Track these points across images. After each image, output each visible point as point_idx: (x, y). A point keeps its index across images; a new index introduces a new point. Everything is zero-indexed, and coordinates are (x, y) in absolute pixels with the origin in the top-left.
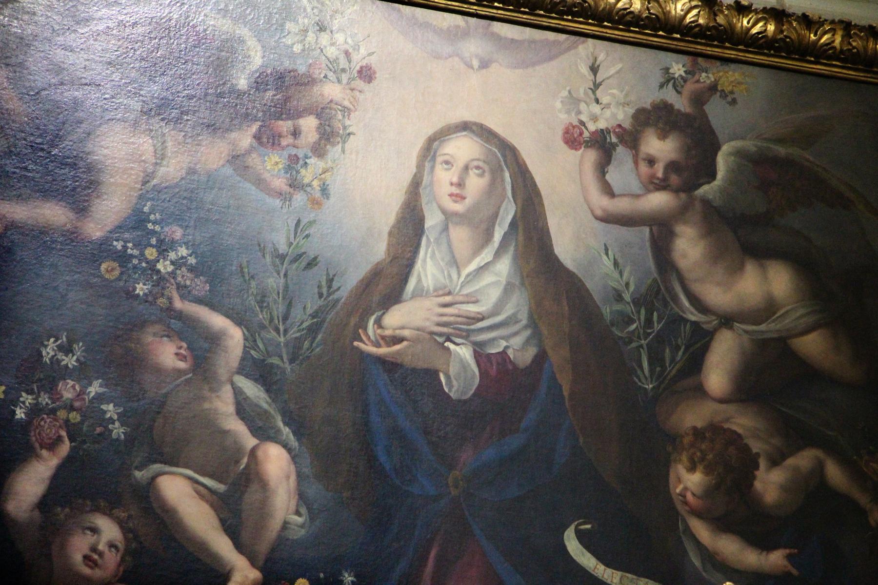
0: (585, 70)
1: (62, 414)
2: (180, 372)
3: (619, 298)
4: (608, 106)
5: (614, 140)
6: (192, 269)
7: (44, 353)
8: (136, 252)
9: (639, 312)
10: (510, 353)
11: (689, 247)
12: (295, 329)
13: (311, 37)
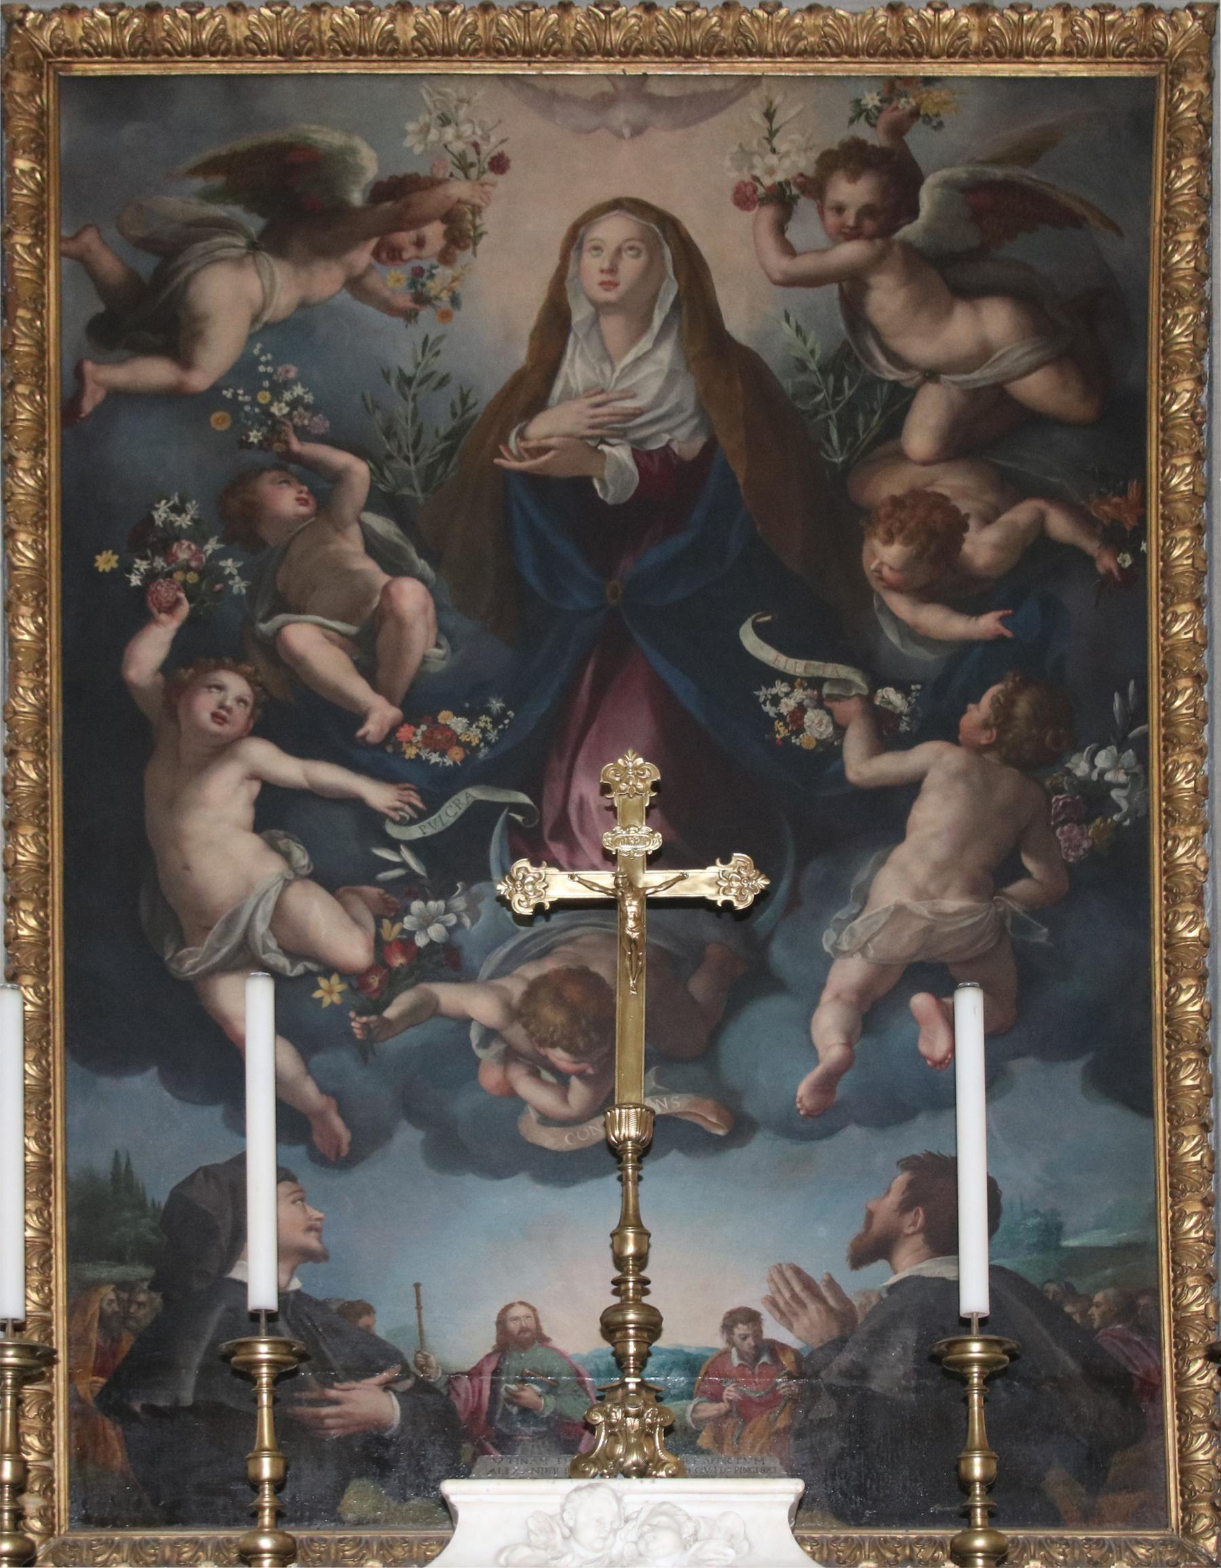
0: (758, 118)
1: (179, 576)
2: (304, 518)
3: (802, 366)
4: (787, 154)
5: (795, 191)
6: (307, 407)
7: (156, 517)
8: (247, 398)
9: (826, 381)
10: (675, 447)
11: (886, 299)
12: (427, 455)
13: (433, 135)
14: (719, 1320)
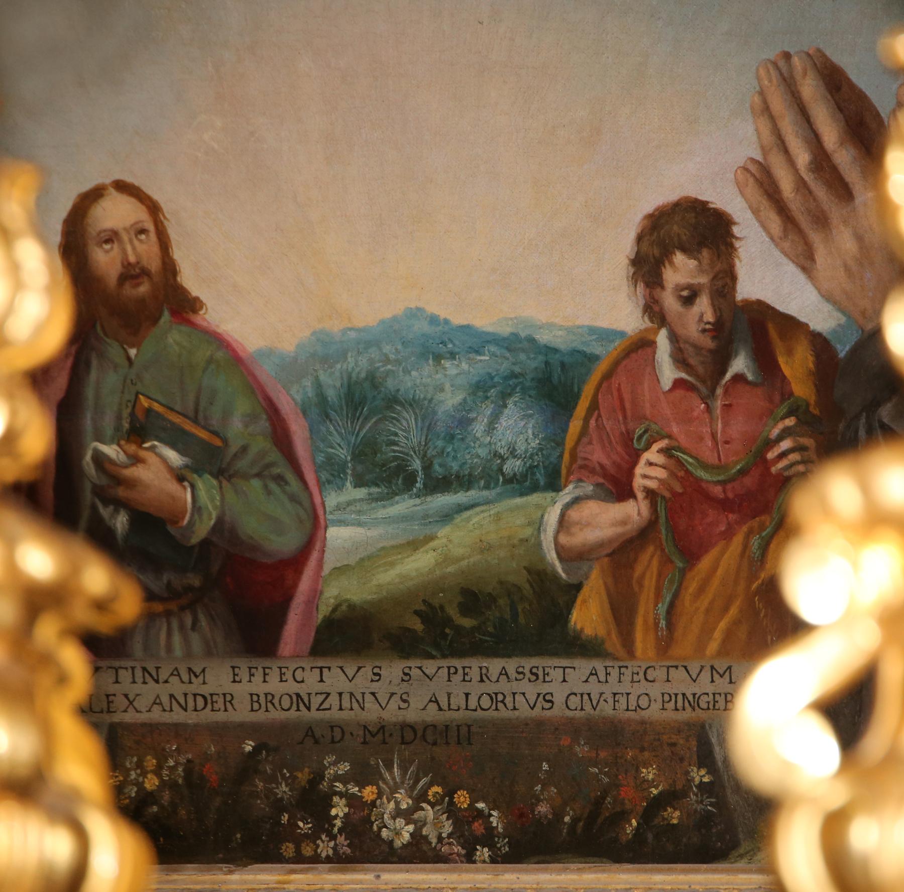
14: (623, 244)
